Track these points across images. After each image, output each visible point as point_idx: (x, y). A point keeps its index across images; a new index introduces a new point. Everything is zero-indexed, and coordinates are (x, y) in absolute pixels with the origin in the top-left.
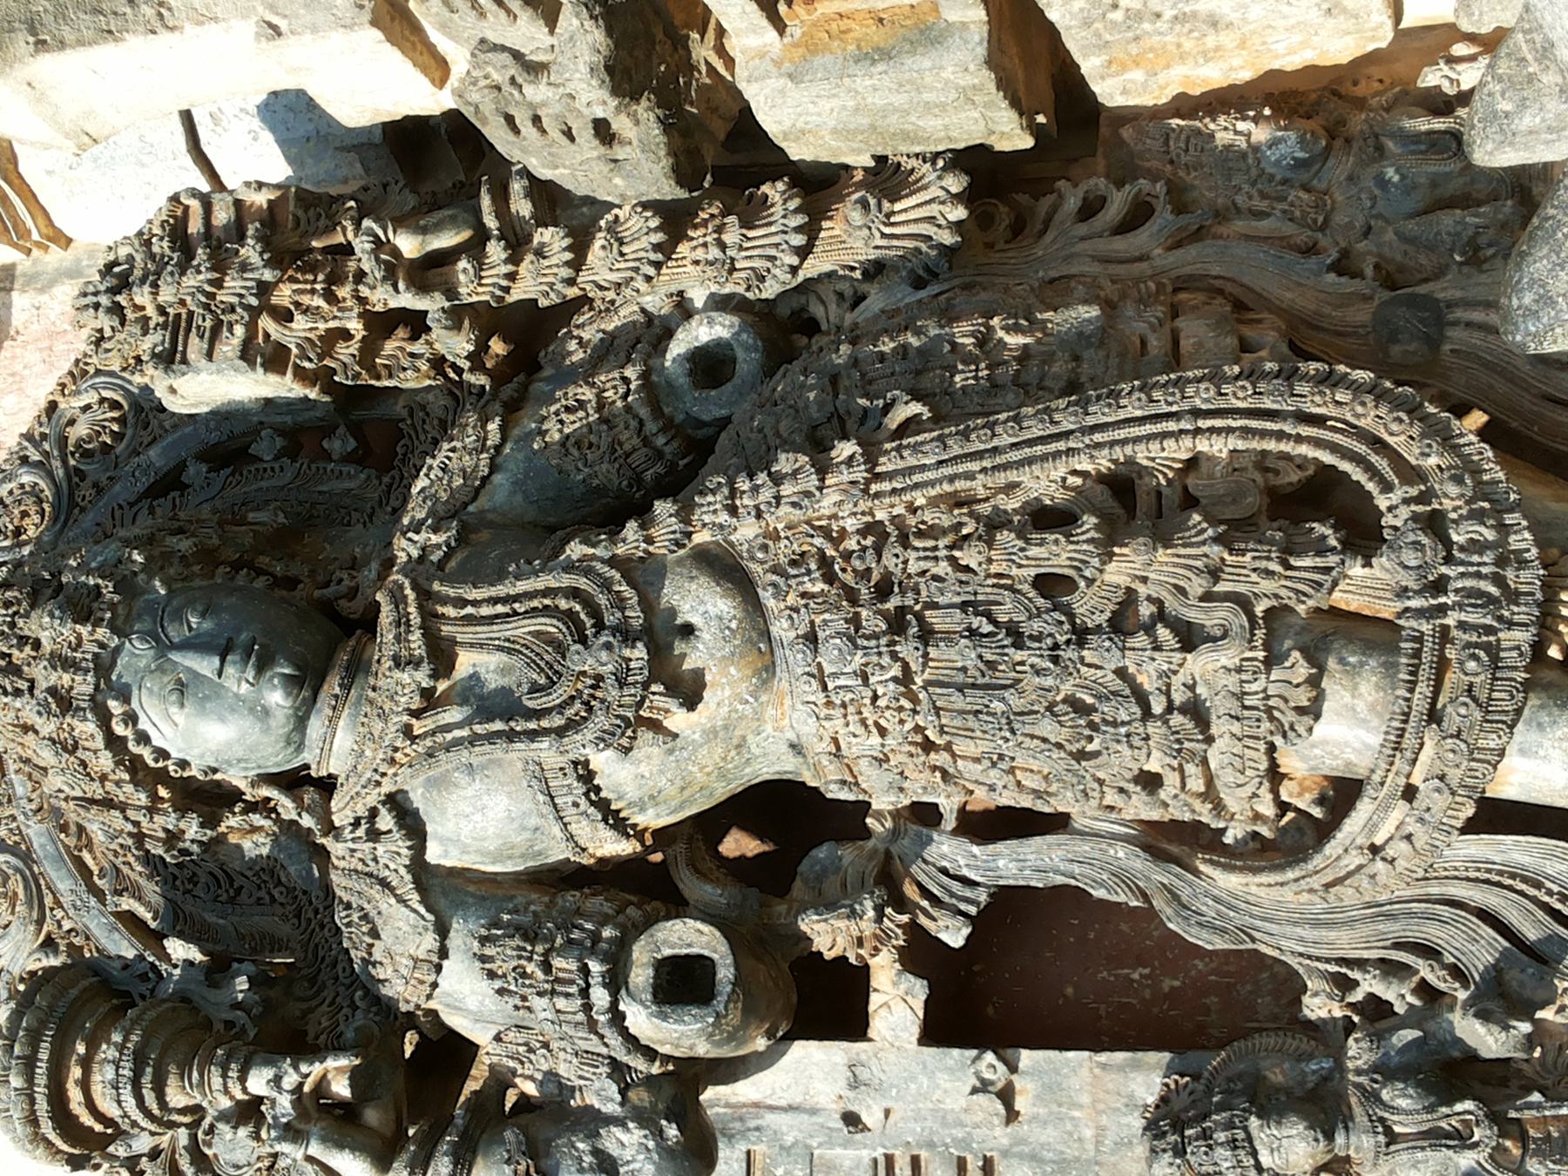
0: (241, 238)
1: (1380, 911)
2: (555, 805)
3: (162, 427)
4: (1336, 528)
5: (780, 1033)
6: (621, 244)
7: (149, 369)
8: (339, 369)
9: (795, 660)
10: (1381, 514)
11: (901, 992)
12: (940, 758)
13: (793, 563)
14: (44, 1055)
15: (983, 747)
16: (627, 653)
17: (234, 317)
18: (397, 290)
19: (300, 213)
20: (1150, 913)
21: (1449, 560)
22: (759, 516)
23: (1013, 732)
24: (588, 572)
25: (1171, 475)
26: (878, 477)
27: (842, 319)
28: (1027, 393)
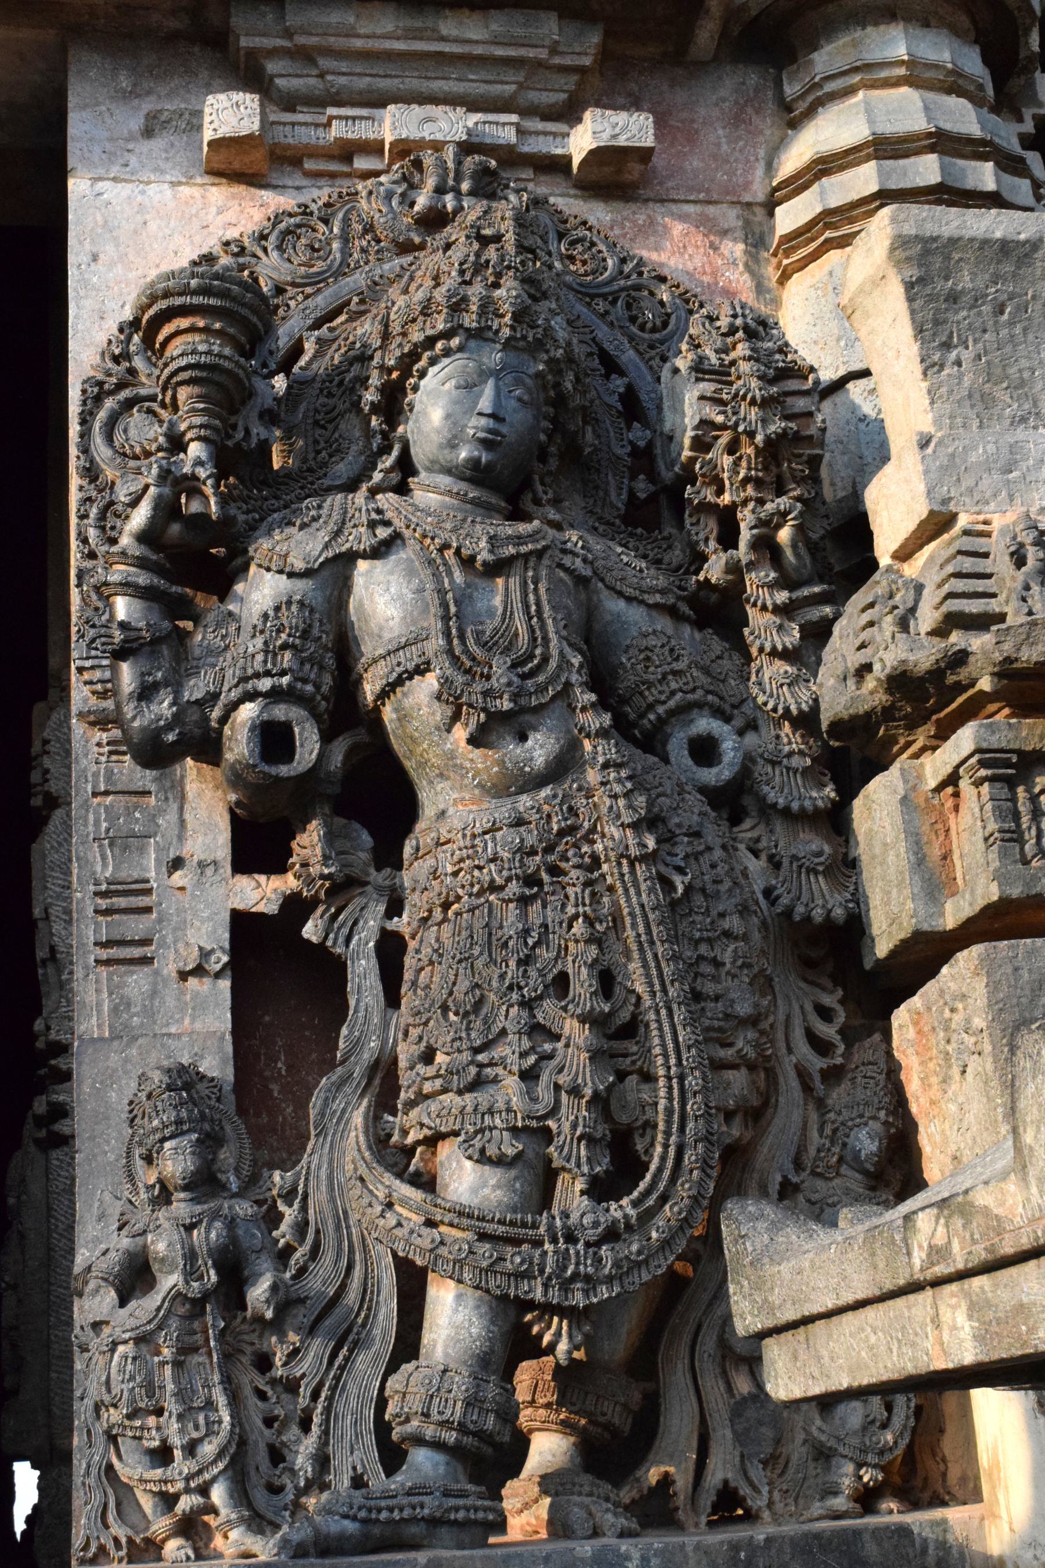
0: (787, 417)
1: (341, 1220)
2: (398, 650)
3: (651, 359)
4: (606, 1172)
5: (238, 811)
6: (789, 685)
7: (691, 356)
8: (695, 489)
9: (503, 811)
10: (617, 1201)
11: (268, 895)
12: (438, 914)
13: (571, 809)
14: (212, 301)
15: (448, 943)
16: (506, 696)
17: (730, 414)
18: (751, 528)
19: (805, 458)
20: (332, 1065)
21: (588, 1245)
22: (603, 784)
23: (460, 961)
24: (559, 667)
25: (639, 1063)
26: (632, 864)
27: (741, 842)
28: (692, 965)
